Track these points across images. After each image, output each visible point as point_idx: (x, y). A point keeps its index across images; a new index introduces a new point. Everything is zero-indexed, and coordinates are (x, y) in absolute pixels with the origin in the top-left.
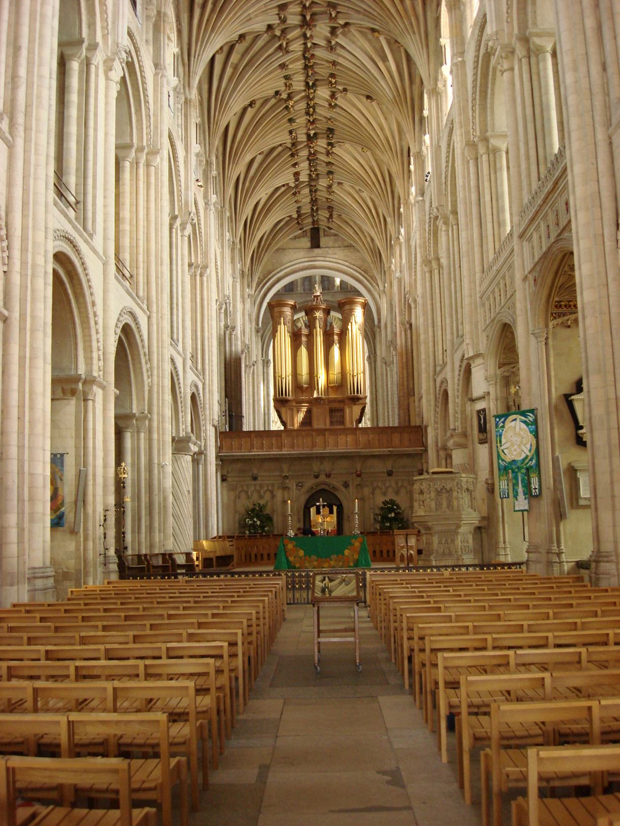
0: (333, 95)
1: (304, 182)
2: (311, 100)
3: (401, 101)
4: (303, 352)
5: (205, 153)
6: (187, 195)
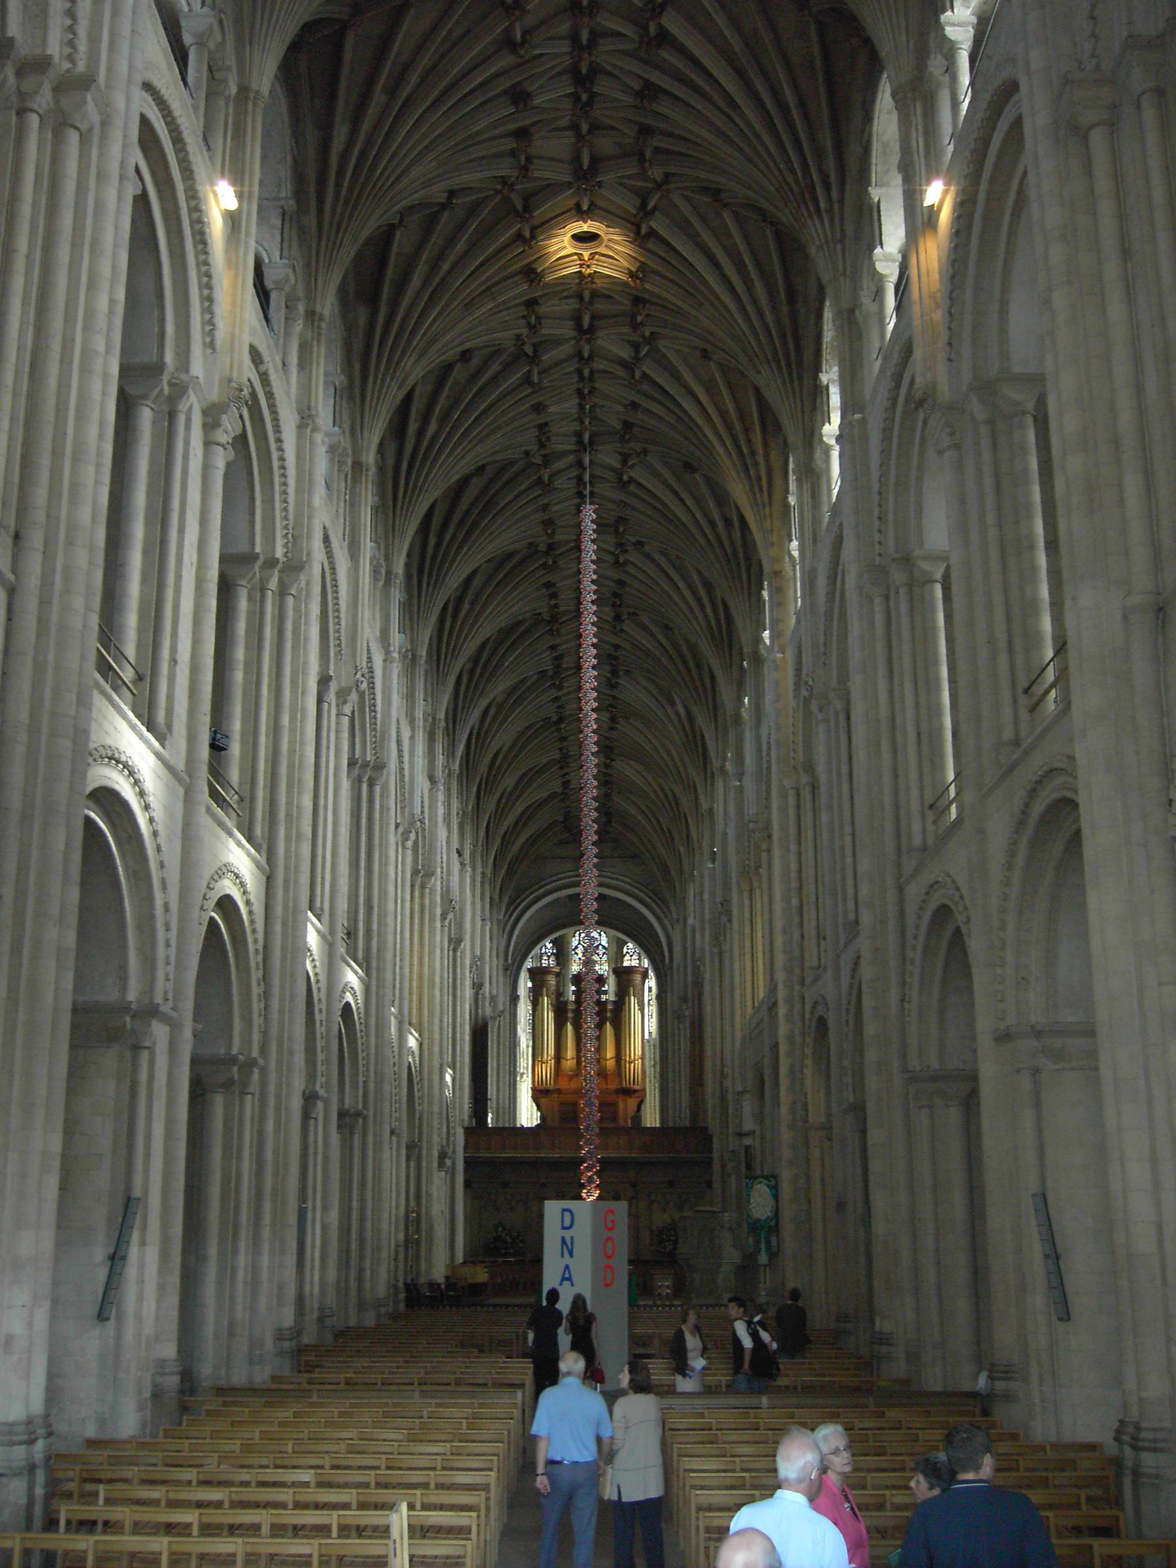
4: (569, 1027)
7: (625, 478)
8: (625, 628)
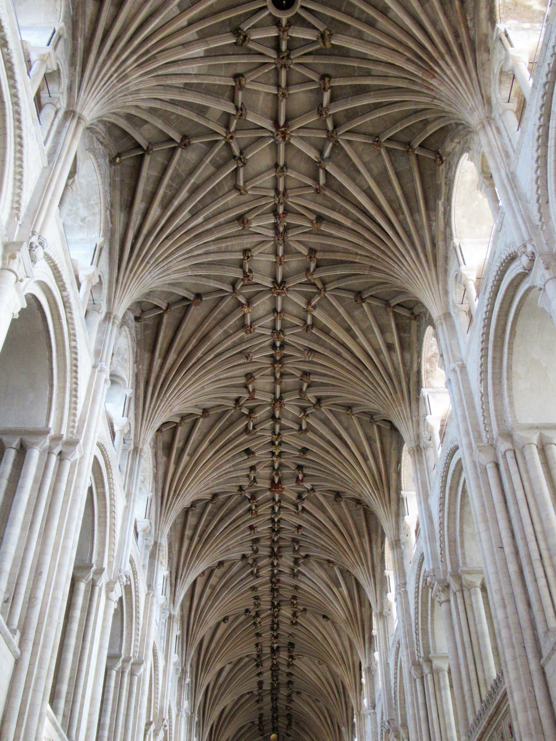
0: (294, 614)
1: (266, 690)
2: (276, 617)
3: (352, 621)
5: (182, 662)
6: (162, 702)
7: (309, 322)
8: (298, 621)
